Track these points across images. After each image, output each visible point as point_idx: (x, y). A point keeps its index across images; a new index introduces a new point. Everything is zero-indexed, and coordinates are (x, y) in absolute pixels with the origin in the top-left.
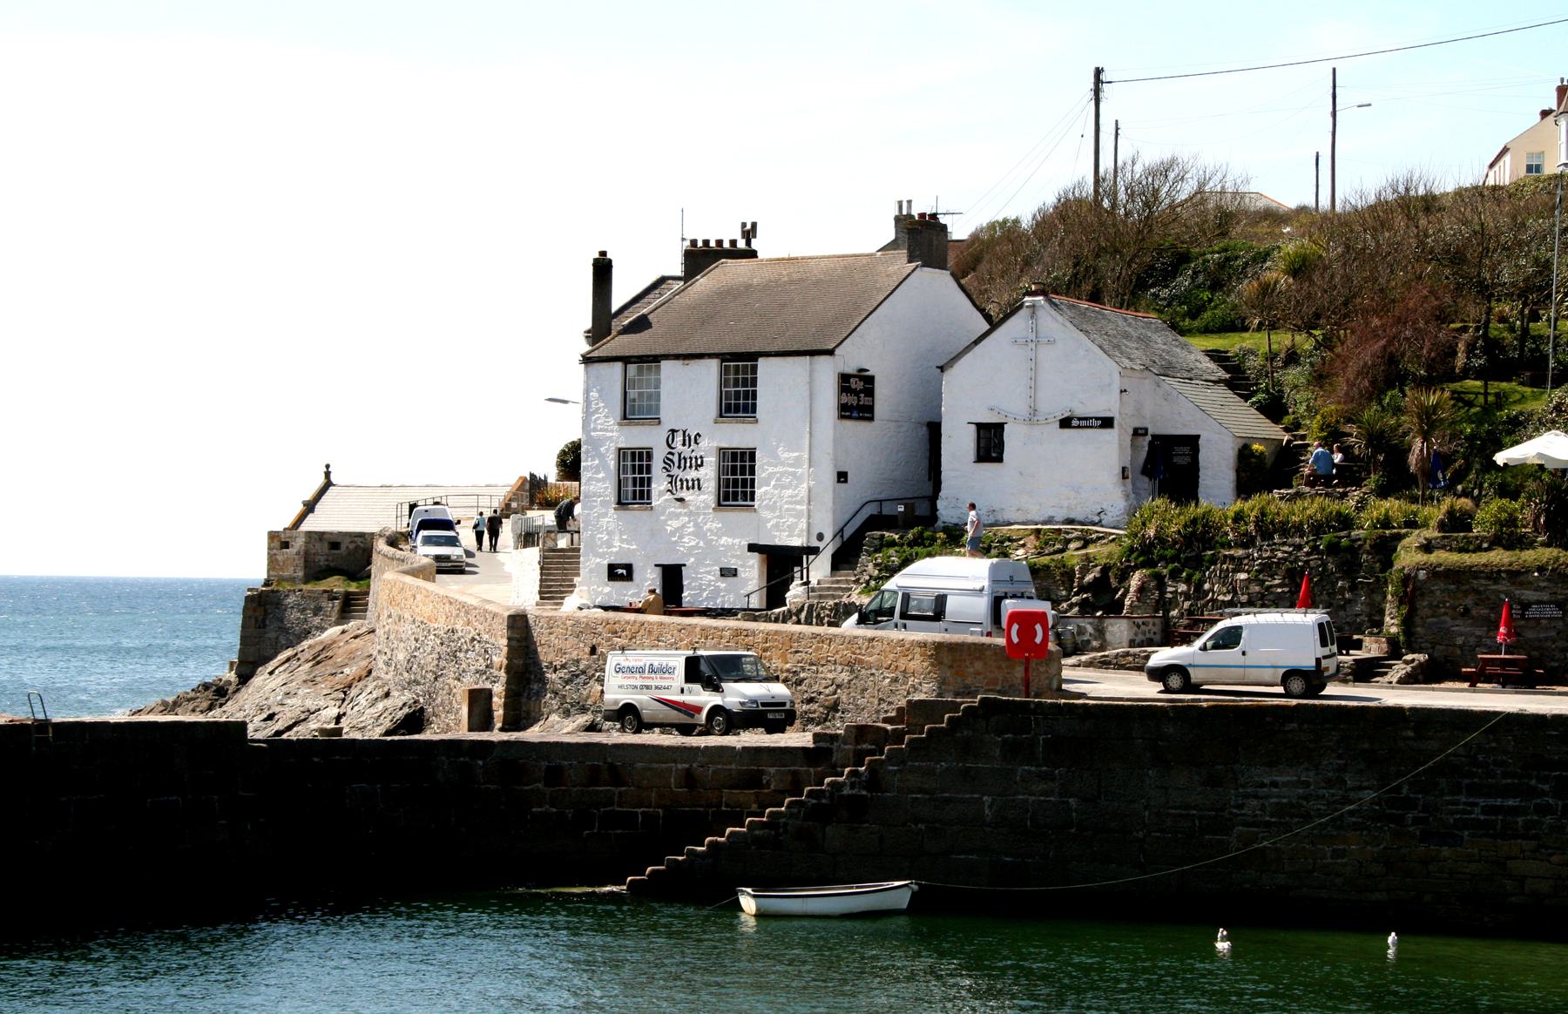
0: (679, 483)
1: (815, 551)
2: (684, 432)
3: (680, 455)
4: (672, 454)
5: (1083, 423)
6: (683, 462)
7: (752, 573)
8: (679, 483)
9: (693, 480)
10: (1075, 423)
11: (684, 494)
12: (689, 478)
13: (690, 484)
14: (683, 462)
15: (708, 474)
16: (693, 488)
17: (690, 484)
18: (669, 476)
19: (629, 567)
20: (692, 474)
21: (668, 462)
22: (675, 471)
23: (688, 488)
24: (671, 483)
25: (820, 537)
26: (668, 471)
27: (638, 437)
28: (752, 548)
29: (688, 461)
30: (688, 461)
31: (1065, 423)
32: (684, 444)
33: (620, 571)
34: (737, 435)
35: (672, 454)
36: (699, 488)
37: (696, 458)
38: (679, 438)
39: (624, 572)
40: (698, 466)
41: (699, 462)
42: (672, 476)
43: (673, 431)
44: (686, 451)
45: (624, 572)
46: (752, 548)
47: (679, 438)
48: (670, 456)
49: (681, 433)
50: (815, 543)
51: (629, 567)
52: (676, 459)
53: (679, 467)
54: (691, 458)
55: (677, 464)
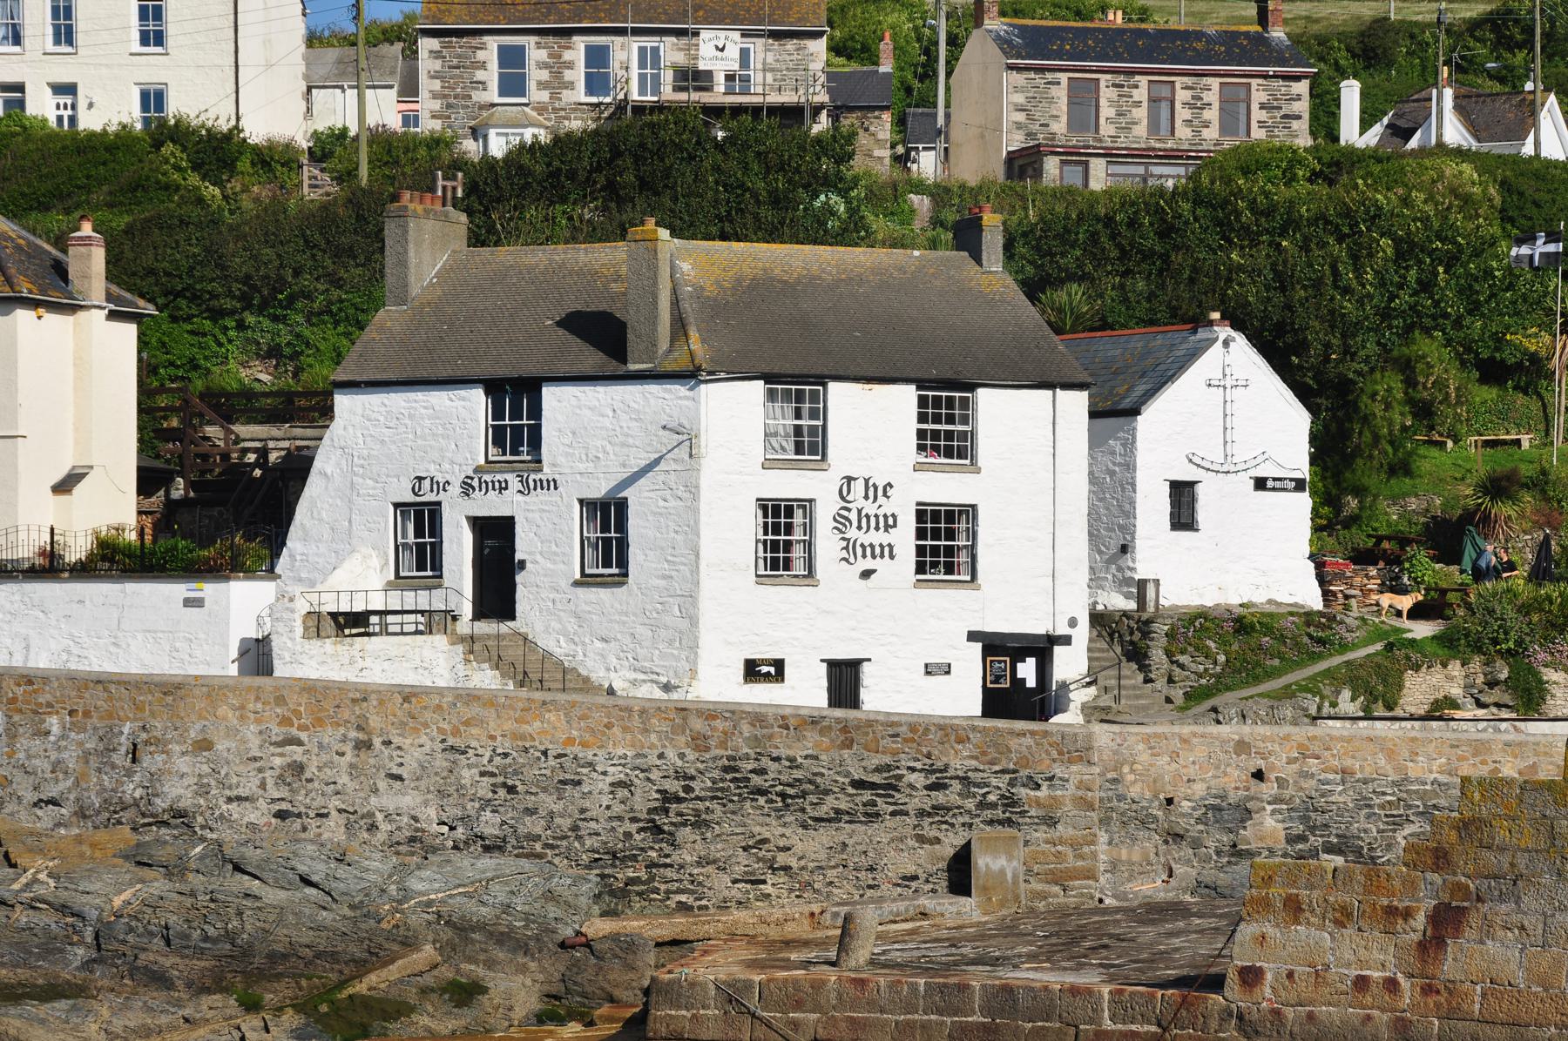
0: (859, 551)
1: (1066, 640)
2: (867, 481)
3: (860, 511)
4: (849, 510)
5: (1278, 484)
6: (864, 521)
7: (970, 665)
8: (859, 551)
9: (881, 546)
10: (1270, 484)
11: (869, 564)
12: (876, 543)
13: (878, 550)
14: (864, 521)
15: (905, 538)
16: (882, 556)
17: (878, 550)
18: (843, 539)
19: (779, 664)
20: (877, 537)
21: (841, 521)
22: (852, 533)
23: (874, 557)
24: (846, 548)
25: (1073, 623)
26: (841, 532)
27: (788, 485)
28: (973, 636)
29: (873, 520)
30: (873, 520)
31: (1260, 484)
32: (866, 497)
33: (765, 669)
34: (946, 487)
35: (849, 510)
36: (892, 557)
37: (885, 516)
38: (858, 486)
39: (772, 670)
40: (887, 527)
41: (891, 521)
42: (849, 540)
43: (850, 479)
44: (870, 508)
45: (772, 670)
46: (973, 636)
47: (858, 486)
48: (842, 512)
49: (861, 483)
50: (1062, 630)
51: (779, 664)
52: (853, 516)
53: (859, 528)
54: (876, 516)
55: (855, 524)
